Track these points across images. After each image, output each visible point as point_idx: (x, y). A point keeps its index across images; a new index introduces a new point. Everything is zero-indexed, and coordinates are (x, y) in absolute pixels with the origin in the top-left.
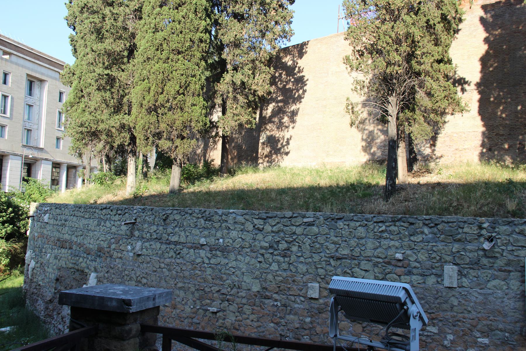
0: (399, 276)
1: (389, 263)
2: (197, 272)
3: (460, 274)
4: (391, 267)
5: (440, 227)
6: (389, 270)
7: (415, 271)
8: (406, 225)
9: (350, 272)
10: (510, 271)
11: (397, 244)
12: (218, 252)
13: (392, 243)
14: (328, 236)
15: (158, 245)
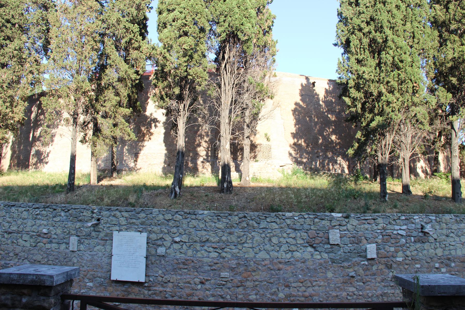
0: (45, 244)
1: (39, 236)
3: (80, 242)
4: (40, 238)
5: (70, 212)
6: (39, 240)
7: (54, 241)
8: (51, 210)
9: (16, 242)
10: (107, 240)
11: (45, 223)
13: (43, 222)
14: (5, 218)
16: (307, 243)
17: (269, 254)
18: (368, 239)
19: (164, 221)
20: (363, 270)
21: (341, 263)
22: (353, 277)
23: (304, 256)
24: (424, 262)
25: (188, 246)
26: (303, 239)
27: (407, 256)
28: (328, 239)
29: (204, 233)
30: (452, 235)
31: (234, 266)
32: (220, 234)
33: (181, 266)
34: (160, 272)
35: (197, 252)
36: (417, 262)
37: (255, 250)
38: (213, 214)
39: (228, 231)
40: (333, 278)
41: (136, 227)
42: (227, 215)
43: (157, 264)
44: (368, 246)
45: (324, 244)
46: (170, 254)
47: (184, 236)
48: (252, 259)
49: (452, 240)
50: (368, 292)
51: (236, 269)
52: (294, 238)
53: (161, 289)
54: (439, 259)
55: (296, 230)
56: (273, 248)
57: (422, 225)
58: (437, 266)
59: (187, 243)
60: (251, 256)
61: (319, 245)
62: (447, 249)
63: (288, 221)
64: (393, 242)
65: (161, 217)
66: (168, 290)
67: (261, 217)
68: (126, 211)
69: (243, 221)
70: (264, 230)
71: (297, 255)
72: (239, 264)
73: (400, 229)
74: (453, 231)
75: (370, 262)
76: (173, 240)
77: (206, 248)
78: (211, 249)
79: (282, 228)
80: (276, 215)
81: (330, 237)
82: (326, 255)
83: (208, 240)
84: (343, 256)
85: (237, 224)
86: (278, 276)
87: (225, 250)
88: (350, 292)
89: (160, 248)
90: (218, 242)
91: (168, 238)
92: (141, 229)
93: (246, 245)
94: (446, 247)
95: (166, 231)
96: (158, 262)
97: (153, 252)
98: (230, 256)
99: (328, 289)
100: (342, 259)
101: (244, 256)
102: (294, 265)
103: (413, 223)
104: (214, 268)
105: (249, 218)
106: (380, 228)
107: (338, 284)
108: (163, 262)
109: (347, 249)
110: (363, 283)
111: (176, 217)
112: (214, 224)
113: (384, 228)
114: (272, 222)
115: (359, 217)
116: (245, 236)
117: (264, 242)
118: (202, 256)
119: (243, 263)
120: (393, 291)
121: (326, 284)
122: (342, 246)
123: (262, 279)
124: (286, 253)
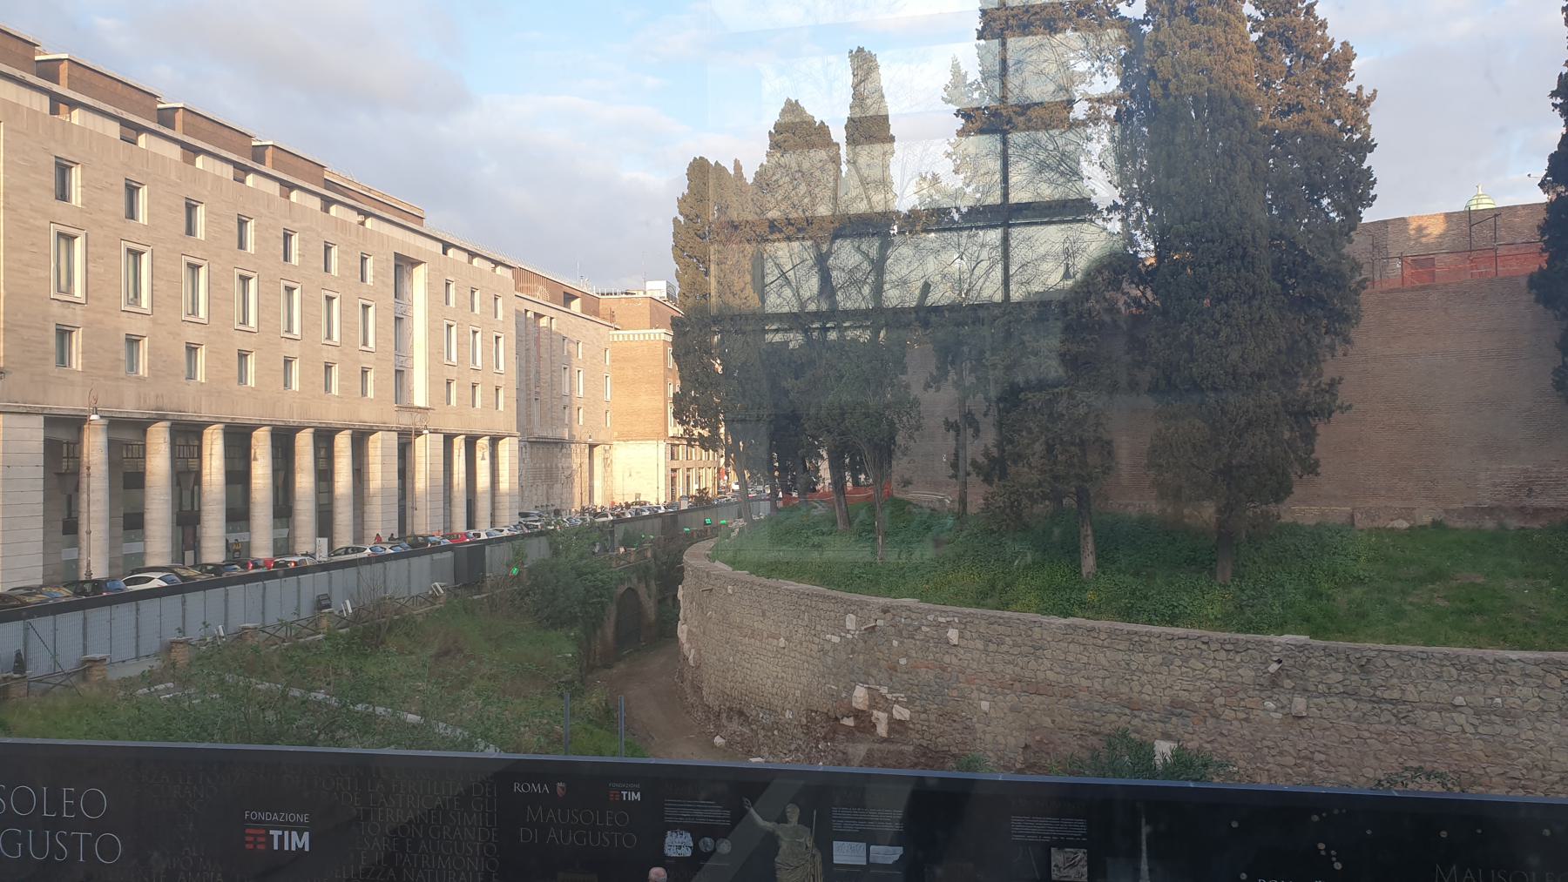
2: (1451, 745)
12: (1493, 717)
15: (1351, 704)
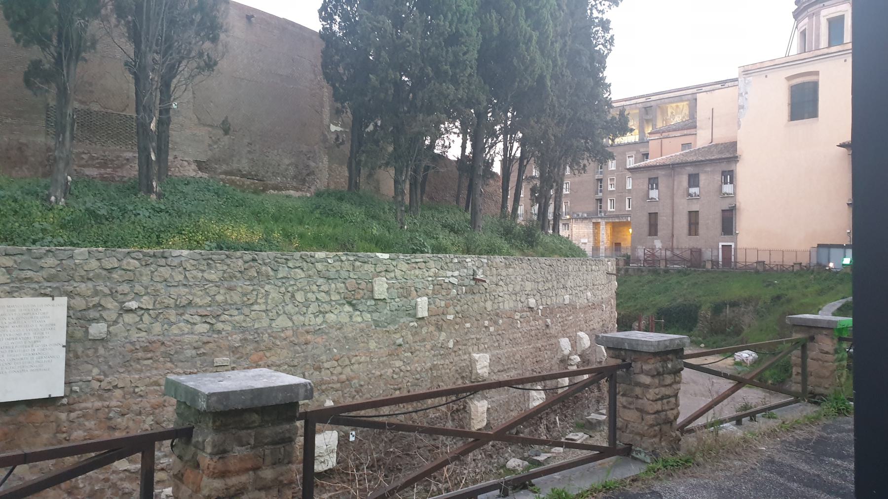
16: (344, 298)
17: (291, 319)
18: (418, 290)
19: (101, 271)
20: (412, 335)
21: (386, 327)
22: (400, 345)
23: (340, 319)
24: (474, 319)
25: (153, 316)
26: (339, 293)
27: (457, 313)
28: (372, 291)
29: (183, 290)
30: (501, 283)
31: (237, 345)
32: (213, 290)
33: (140, 354)
34: (95, 371)
35: (171, 326)
36: (467, 319)
37: (270, 314)
38: (199, 257)
39: (226, 284)
40: (376, 350)
41: (37, 286)
42: (223, 257)
43: (88, 356)
44: (419, 300)
45: (366, 299)
46: (116, 335)
47: (145, 297)
48: (266, 330)
49: (500, 289)
50: (417, 365)
51: (240, 349)
52: (327, 293)
53: (98, 404)
54: (489, 315)
55: (329, 279)
56: (297, 309)
57: (474, 270)
58: (486, 325)
59: (151, 312)
60: (266, 325)
61: (360, 302)
62: (496, 301)
63: (319, 266)
64: (444, 294)
65: (94, 264)
66: (114, 403)
67: (279, 260)
68: (6, 255)
69: (252, 267)
70: (284, 281)
71: (331, 319)
72: (246, 339)
73: (452, 276)
74: (502, 278)
75: (419, 323)
76: (122, 309)
77: (187, 317)
78: (198, 318)
79: (310, 276)
80: (301, 257)
81: (376, 288)
82: (369, 316)
83: (190, 303)
84: (389, 315)
85: (240, 272)
86: (305, 354)
87: (223, 318)
88: (396, 367)
89: (94, 325)
90: (210, 306)
91: (110, 304)
92: (49, 289)
93: (256, 307)
94: (495, 298)
95: (107, 291)
96: (90, 352)
97: (79, 334)
98: (229, 328)
99: (370, 366)
100: (388, 321)
101: (254, 325)
102: (326, 334)
103: (465, 268)
104: (202, 350)
105: (261, 262)
106: (432, 274)
107: (382, 357)
108: (101, 351)
109: (394, 305)
110: (411, 353)
111: (129, 263)
112: (200, 275)
113: (436, 275)
114: (296, 268)
115: (409, 260)
116: (255, 293)
117: (284, 301)
118: (181, 333)
119: (251, 337)
120: (442, 362)
121: (368, 359)
122: (388, 301)
123: (282, 362)
124: (315, 317)
